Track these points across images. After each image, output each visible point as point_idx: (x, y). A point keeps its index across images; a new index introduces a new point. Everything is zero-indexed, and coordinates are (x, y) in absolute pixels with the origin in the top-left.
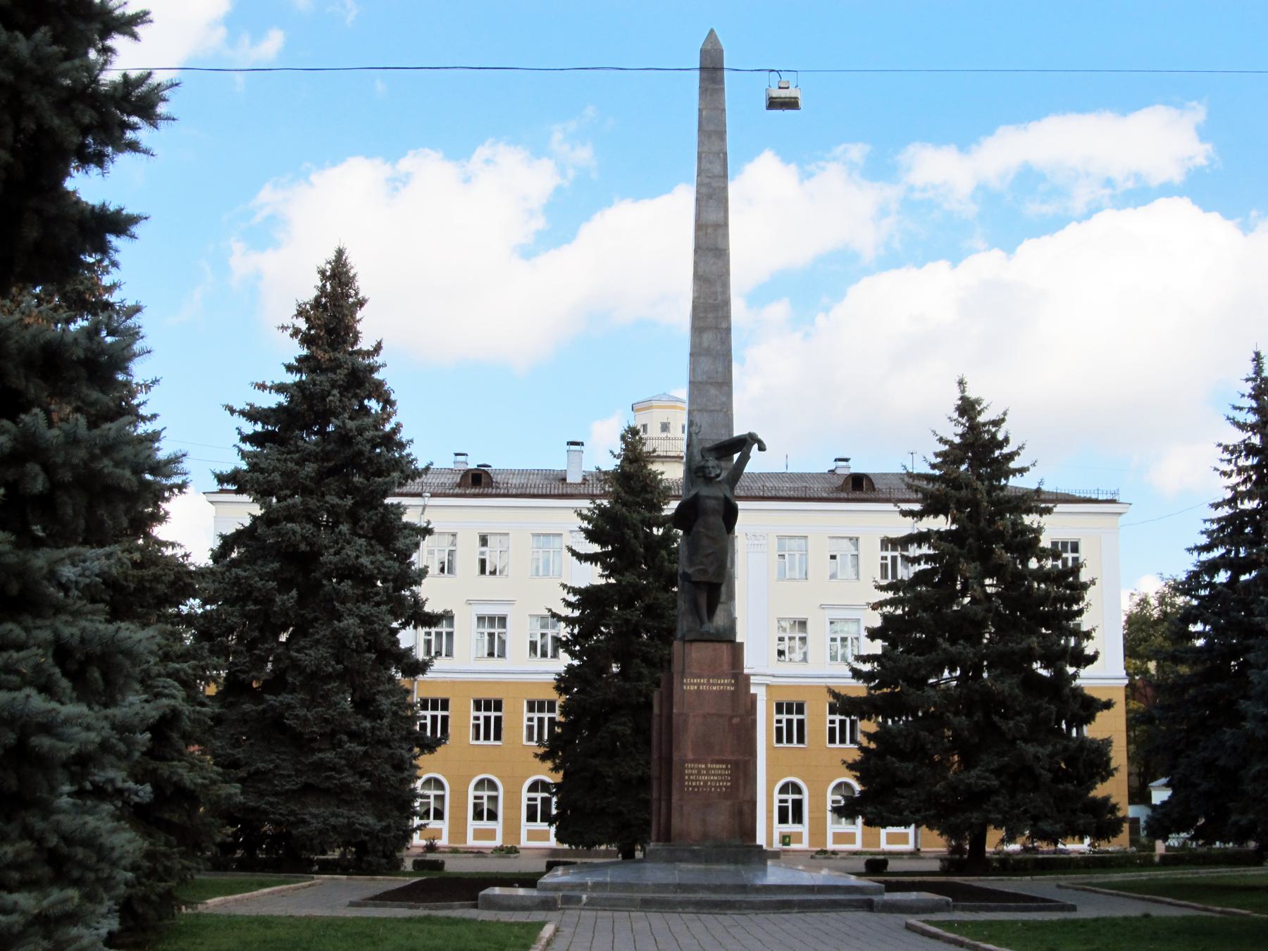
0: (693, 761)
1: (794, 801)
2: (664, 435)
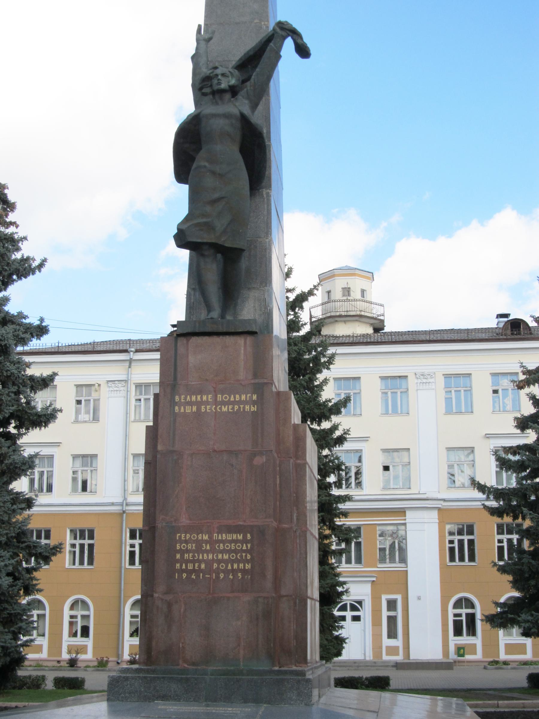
0: (188, 529)
1: (467, 615)
2: (345, 298)
